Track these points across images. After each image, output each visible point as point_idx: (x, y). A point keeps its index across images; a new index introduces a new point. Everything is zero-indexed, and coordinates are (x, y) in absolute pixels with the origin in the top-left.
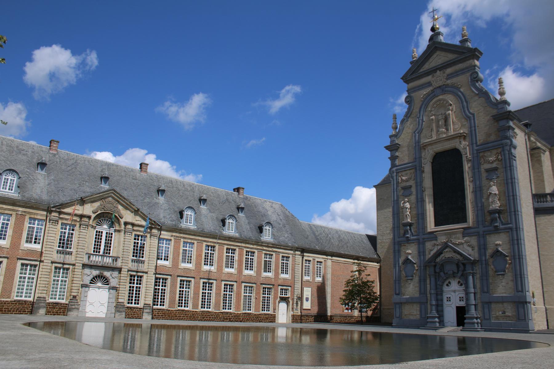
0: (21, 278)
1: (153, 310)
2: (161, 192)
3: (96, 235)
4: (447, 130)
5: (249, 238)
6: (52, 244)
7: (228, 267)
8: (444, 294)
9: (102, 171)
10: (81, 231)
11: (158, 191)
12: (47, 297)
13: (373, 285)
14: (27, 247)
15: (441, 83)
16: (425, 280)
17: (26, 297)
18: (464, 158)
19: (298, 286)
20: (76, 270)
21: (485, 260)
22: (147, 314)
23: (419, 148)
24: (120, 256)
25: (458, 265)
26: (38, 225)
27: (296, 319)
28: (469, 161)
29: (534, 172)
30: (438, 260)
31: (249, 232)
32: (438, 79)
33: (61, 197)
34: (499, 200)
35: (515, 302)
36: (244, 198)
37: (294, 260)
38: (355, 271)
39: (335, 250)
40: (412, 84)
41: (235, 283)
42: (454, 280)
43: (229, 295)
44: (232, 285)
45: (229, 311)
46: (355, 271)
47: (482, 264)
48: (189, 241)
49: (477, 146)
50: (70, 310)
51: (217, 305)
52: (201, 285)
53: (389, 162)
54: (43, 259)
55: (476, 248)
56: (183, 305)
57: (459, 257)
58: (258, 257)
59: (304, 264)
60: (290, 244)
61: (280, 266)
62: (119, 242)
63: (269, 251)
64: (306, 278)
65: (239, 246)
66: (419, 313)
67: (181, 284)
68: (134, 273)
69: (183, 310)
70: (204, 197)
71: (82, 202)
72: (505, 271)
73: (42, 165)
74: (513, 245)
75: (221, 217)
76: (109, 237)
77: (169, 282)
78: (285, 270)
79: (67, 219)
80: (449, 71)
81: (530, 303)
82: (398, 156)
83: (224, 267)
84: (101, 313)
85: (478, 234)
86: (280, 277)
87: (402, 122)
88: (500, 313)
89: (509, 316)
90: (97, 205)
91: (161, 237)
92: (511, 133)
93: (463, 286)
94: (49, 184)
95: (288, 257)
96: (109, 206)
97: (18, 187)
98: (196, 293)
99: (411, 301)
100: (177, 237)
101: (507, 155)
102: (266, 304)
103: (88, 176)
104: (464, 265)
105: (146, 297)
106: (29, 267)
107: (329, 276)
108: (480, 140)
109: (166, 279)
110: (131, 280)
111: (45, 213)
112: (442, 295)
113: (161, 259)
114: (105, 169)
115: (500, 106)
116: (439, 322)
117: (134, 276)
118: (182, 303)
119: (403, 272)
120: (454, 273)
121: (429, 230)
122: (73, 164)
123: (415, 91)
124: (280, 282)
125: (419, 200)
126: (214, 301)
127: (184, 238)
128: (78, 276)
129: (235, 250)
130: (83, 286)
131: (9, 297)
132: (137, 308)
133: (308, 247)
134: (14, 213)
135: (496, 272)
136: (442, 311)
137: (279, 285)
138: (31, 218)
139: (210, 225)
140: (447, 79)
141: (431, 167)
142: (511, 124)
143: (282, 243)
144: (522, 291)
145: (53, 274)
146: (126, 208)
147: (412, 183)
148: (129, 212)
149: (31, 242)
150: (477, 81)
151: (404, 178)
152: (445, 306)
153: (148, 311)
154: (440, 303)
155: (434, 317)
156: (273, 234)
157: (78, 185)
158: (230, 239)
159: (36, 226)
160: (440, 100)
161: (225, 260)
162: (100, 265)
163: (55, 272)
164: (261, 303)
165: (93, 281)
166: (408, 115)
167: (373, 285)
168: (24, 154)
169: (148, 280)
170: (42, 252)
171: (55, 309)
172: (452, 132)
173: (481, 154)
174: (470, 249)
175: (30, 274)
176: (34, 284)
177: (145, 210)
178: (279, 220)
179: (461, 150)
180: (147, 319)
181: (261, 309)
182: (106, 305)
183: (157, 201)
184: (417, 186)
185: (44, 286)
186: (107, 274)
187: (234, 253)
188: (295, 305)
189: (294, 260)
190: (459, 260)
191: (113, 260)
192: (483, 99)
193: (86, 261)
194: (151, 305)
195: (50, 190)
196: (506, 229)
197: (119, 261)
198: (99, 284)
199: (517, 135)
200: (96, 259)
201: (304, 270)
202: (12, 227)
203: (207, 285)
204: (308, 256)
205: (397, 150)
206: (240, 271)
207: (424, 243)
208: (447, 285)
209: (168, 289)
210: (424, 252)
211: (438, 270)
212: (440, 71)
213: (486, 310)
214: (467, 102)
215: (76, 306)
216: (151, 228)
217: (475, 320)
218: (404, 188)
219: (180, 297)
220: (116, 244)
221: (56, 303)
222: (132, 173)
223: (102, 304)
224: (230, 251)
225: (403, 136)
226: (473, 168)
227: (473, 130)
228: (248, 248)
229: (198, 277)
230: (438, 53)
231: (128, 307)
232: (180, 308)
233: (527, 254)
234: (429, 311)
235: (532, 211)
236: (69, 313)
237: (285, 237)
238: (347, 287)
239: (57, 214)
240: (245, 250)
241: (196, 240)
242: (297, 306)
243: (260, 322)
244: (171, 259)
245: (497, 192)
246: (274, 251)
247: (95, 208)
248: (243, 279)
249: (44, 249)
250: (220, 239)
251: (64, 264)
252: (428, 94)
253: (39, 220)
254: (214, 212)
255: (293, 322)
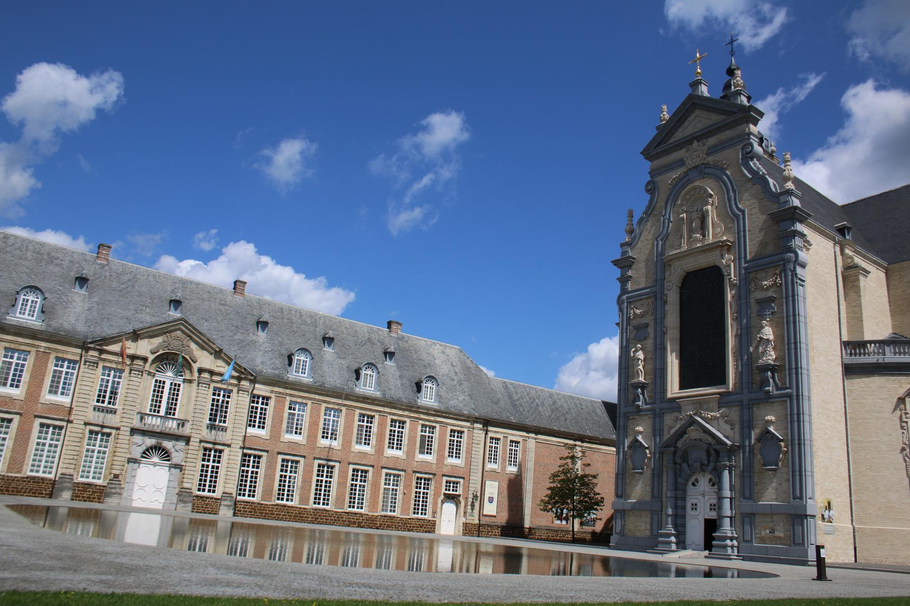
0: (38, 444)
1: (236, 502)
2: (263, 324)
3: (155, 386)
4: (704, 236)
5: (398, 400)
6: (87, 396)
7: (361, 443)
8: (688, 498)
9: (173, 291)
10: (132, 379)
11: (258, 323)
12: (75, 474)
13: (595, 481)
14: (50, 400)
15: (698, 161)
16: (660, 476)
17: (44, 472)
18: (727, 282)
19: (476, 478)
20: (120, 437)
21: (750, 446)
22: (226, 508)
23: (662, 264)
24: (190, 418)
25: (708, 453)
26: (68, 368)
27: (468, 529)
28: (733, 286)
29: (848, 305)
30: (680, 444)
31: (398, 389)
32: (694, 155)
33: (105, 329)
34: (774, 349)
35: (791, 515)
36: (398, 338)
37: (471, 438)
38: (567, 458)
39: (543, 424)
40: (658, 163)
41: (370, 469)
42: (704, 476)
43: (360, 486)
44: (366, 472)
45: (360, 510)
46: (567, 458)
47: (744, 453)
48: (299, 400)
49: (746, 263)
50: (108, 495)
51: (340, 500)
52: (316, 468)
53: (618, 285)
54: (72, 418)
55: (737, 427)
56: (285, 497)
57: (710, 439)
58: (411, 430)
59: (488, 444)
60: (466, 412)
61: (447, 446)
62: (189, 398)
63: (429, 421)
64: (490, 466)
65: (380, 411)
66: (648, 527)
67: (283, 466)
68: (210, 446)
69: (284, 506)
70: (331, 334)
71: (136, 336)
72: (777, 465)
73: (82, 281)
74: (792, 422)
75: (356, 366)
76: (175, 388)
77: (263, 461)
78: (454, 451)
79: (111, 361)
80: (711, 141)
81: (813, 516)
82: (631, 277)
83: (354, 442)
84: (156, 503)
85: (741, 404)
86: (446, 463)
87: (640, 221)
88: (768, 531)
89: (780, 538)
90: (157, 341)
91: (255, 392)
92: (798, 241)
93: (716, 487)
94: (89, 309)
95: (462, 432)
96: (177, 343)
97: (43, 312)
98: (306, 481)
99: (638, 507)
100: (280, 393)
101: (790, 277)
102: (420, 503)
103: (151, 298)
104: (717, 452)
105: (227, 481)
106: (51, 429)
107: (530, 465)
108: (750, 253)
109: (260, 457)
110: (204, 455)
111: (79, 351)
112: (684, 499)
113: (254, 426)
114: (178, 288)
115: (782, 199)
116: (677, 544)
117: (210, 450)
118: (283, 495)
119: (629, 462)
120: (702, 465)
121: (669, 395)
122: (129, 280)
123: (660, 174)
124: (445, 470)
125: (658, 347)
126: (334, 495)
127: (291, 395)
128: (123, 446)
129: (372, 417)
130: (130, 461)
131: (20, 472)
132: (212, 498)
133: (496, 417)
134: (34, 350)
135: (764, 465)
136: (684, 525)
137: (444, 475)
138: (58, 359)
139: (335, 377)
140: (708, 154)
141: (678, 296)
142: (799, 227)
143: (453, 410)
144: (801, 498)
145: (86, 441)
146: (203, 348)
147: (649, 319)
148: (206, 353)
149: (56, 393)
150: (752, 159)
151: (638, 312)
152: (688, 517)
153: (227, 503)
154: (680, 512)
155: (669, 535)
156: (438, 395)
157: (133, 312)
158: (365, 399)
159: (65, 370)
160: (695, 188)
161: (355, 431)
162: (158, 431)
163: (90, 439)
164: (413, 502)
165: (147, 453)
166: (649, 211)
167: (595, 481)
168: (57, 265)
169: (231, 457)
170: (71, 408)
171: (86, 491)
172: (710, 239)
173: (752, 275)
174: (727, 428)
175: (52, 440)
176: (57, 455)
177: (232, 351)
178: (452, 374)
179: (724, 270)
180: (225, 514)
181: (412, 510)
182: (164, 491)
183: (255, 338)
184: (656, 324)
185: (71, 457)
186: (168, 444)
187: (371, 423)
188: (469, 507)
189: (471, 438)
190: (710, 445)
191: (179, 425)
192: (758, 187)
193: (136, 423)
194: (234, 495)
195: (90, 317)
196: (782, 396)
197: (188, 426)
198: (156, 459)
199: (811, 245)
200: (153, 422)
201: (487, 452)
202: (30, 370)
203: (326, 469)
204: (495, 432)
205: (630, 267)
206: (379, 450)
207: (661, 416)
208: (694, 484)
209: (261, 472)
210: (661, 430)
211: (678, 460)
212: (698, 141)
213: (747, 527)
214: (734, 192)
215: (118, 490)
216: (239, 379)
217: (728, 542)
218: (637, 328)
219: (280, 485)
220: (185, 401)
221: (88, 484)
222: (220, 295)
223: (158, 490)
224: (366, 419)
225: (639, 245)
226: (738, 298)
227: (740, 234)
228: (394, 414)
229: (311, 457)
230: (697, 112)
231: (197, 496)
232: (280, 502)
233: (814, 437)
234: (664, 524)
235: (839, 369)
236: (108, 500)
237: (460, 401)
238: (554, 482)
239: (96, 354)
240: (390, 417)
241: (310, 399)
242: (473, 509)
243: (409, 530)
244: (269, 427)
245: (771, 337)
246: (437, 422)
247: (155, 346)
248: (384, 463)
249: (74, 403)
250: (347, 399)
251: (103, 427)
252: (680, 179)
253: (70, 361)
254: (344, 358)
255: (464, 534)
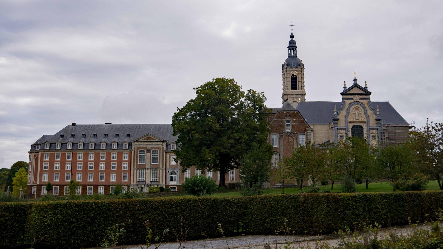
32: (356, 98)
80: (360, 97)
230: (356, 88)
252: (352, 103)
